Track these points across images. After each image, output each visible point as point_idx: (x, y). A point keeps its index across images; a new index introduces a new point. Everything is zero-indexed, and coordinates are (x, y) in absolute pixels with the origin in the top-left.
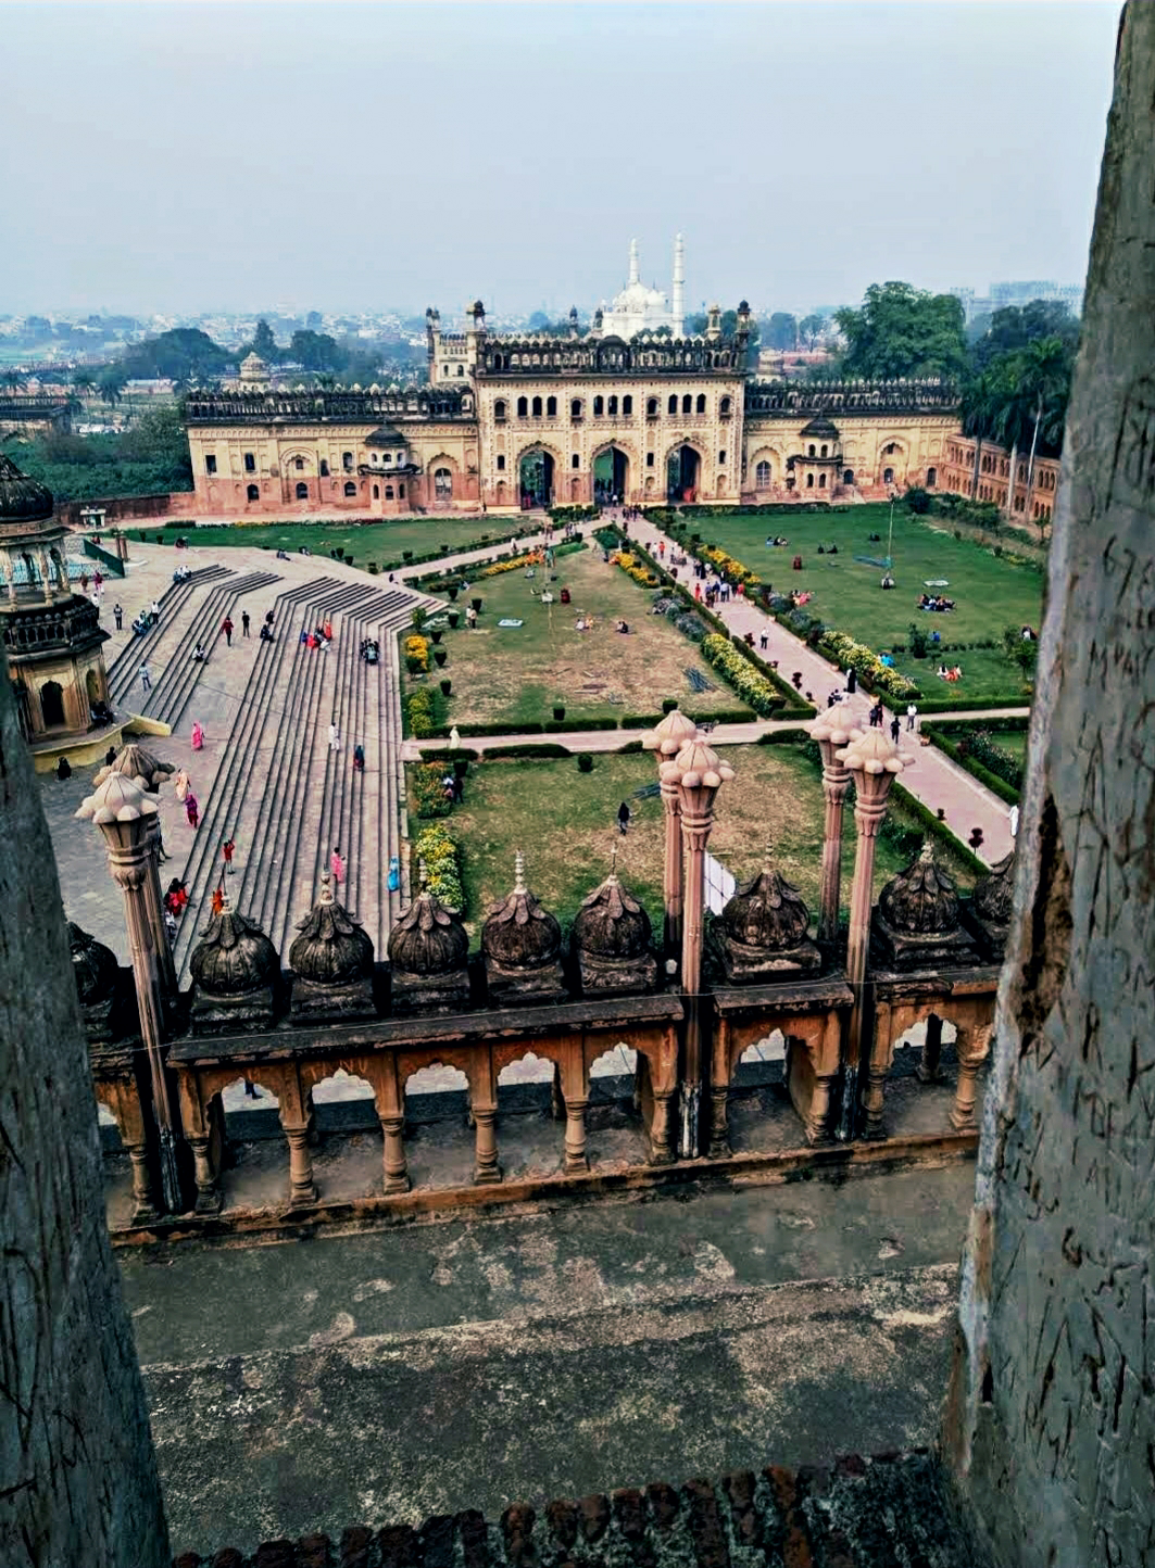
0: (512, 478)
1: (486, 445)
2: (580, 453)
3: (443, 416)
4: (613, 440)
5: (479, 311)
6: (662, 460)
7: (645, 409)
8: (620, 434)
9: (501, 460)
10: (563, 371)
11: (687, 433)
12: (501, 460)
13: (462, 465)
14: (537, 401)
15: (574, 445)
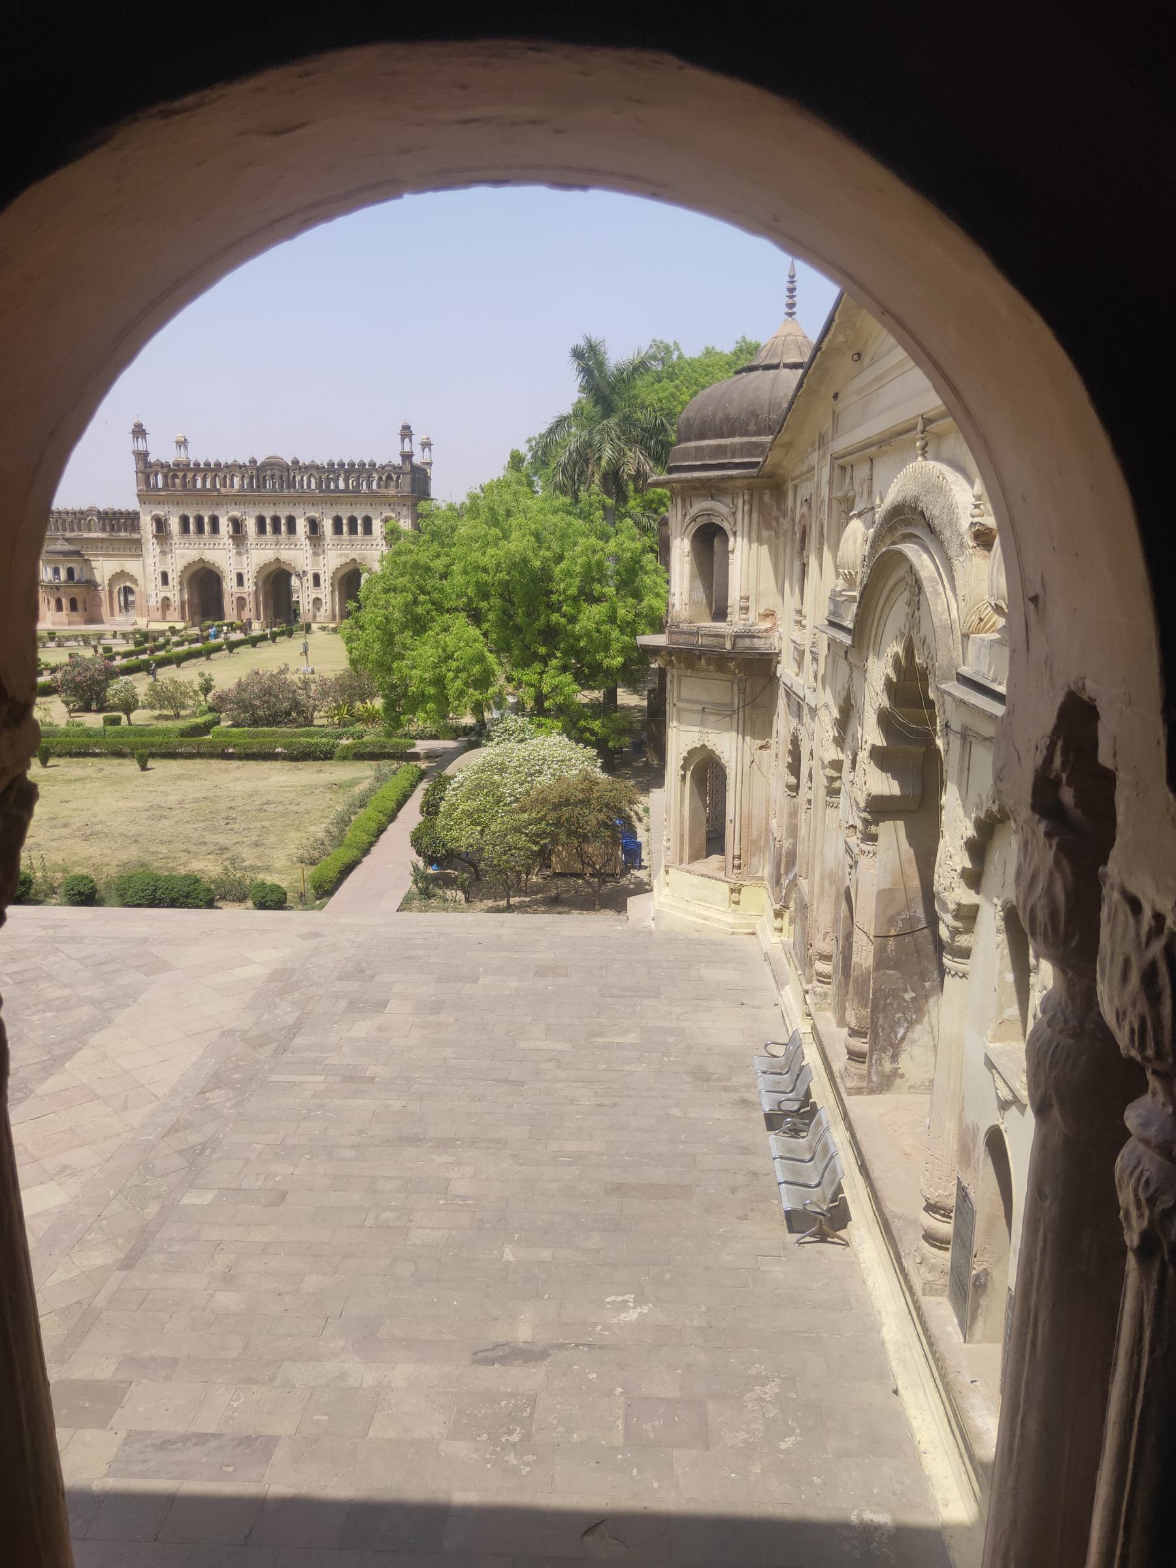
0: (173, 592)
1: (150, 560)
2: (242, 571)
3: (122, 534)
4: (277, 560)
5: (139, 432)
6: (329, 581)
7: (307, 529)
8: (285, 555)
9: (165, 576)
10: (223, 490)
11: (354, 554)
12: (165, 576)
13: (141, 581)
14: (199, 520)
15: (239, 564)
